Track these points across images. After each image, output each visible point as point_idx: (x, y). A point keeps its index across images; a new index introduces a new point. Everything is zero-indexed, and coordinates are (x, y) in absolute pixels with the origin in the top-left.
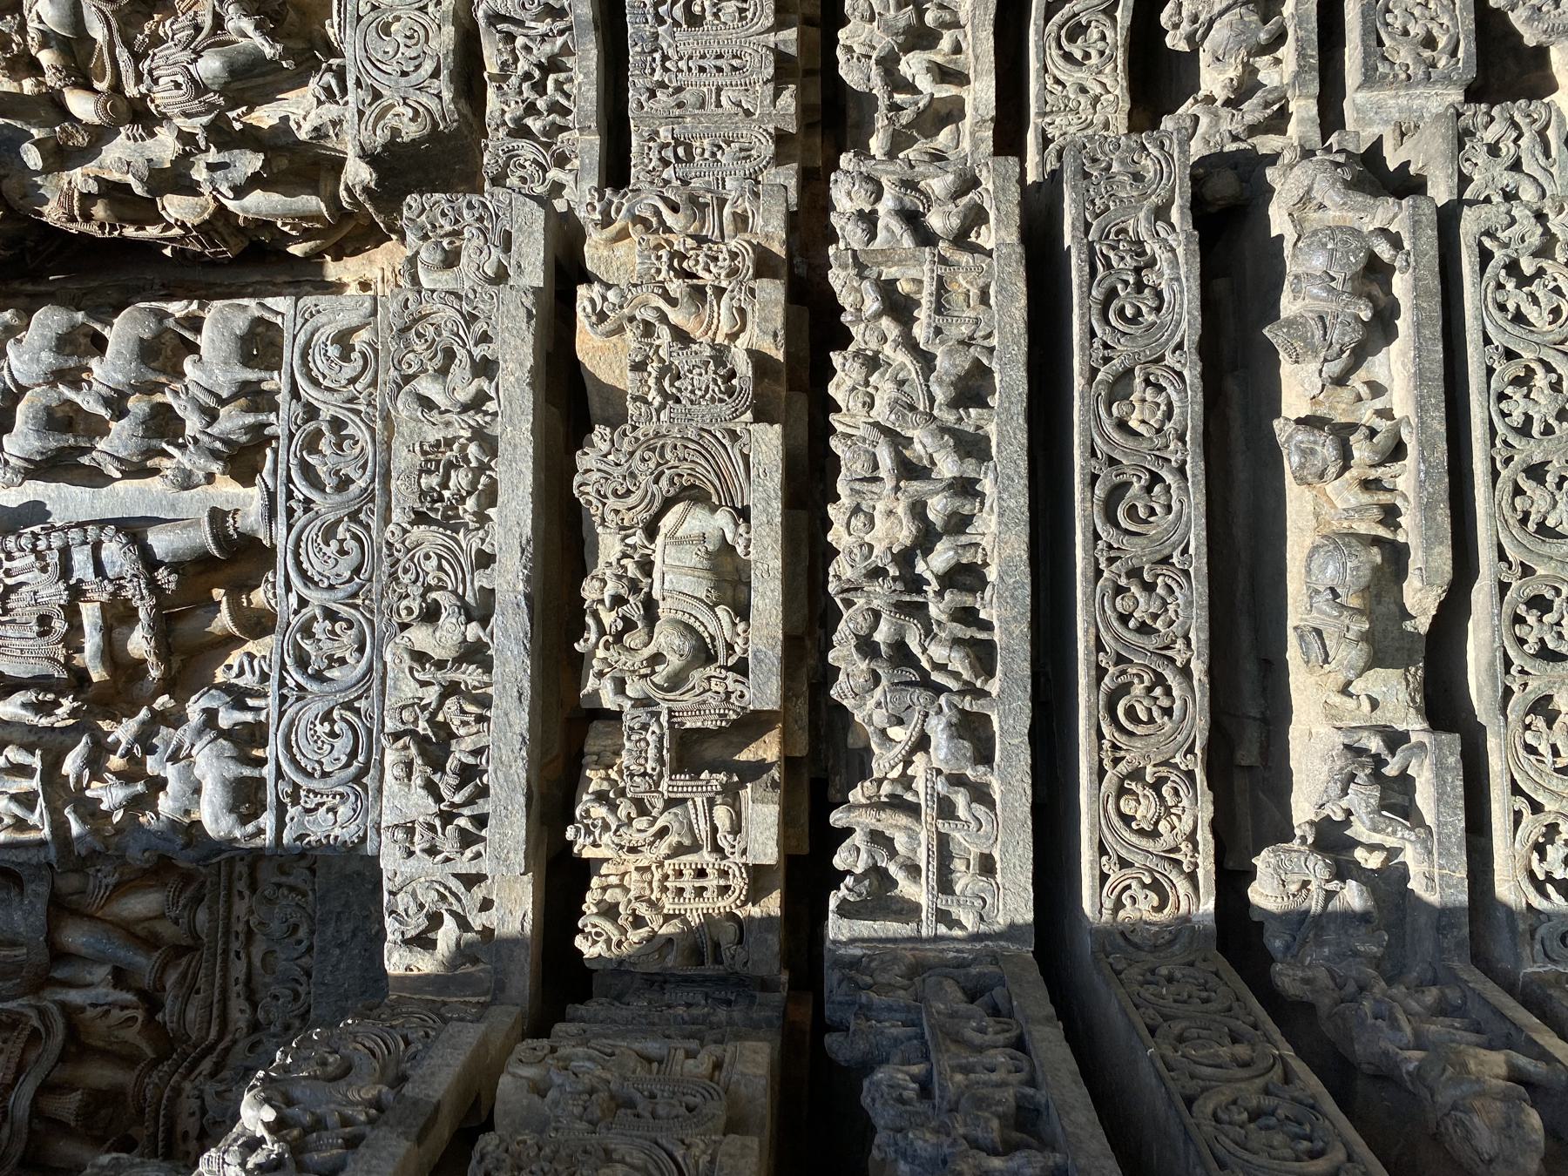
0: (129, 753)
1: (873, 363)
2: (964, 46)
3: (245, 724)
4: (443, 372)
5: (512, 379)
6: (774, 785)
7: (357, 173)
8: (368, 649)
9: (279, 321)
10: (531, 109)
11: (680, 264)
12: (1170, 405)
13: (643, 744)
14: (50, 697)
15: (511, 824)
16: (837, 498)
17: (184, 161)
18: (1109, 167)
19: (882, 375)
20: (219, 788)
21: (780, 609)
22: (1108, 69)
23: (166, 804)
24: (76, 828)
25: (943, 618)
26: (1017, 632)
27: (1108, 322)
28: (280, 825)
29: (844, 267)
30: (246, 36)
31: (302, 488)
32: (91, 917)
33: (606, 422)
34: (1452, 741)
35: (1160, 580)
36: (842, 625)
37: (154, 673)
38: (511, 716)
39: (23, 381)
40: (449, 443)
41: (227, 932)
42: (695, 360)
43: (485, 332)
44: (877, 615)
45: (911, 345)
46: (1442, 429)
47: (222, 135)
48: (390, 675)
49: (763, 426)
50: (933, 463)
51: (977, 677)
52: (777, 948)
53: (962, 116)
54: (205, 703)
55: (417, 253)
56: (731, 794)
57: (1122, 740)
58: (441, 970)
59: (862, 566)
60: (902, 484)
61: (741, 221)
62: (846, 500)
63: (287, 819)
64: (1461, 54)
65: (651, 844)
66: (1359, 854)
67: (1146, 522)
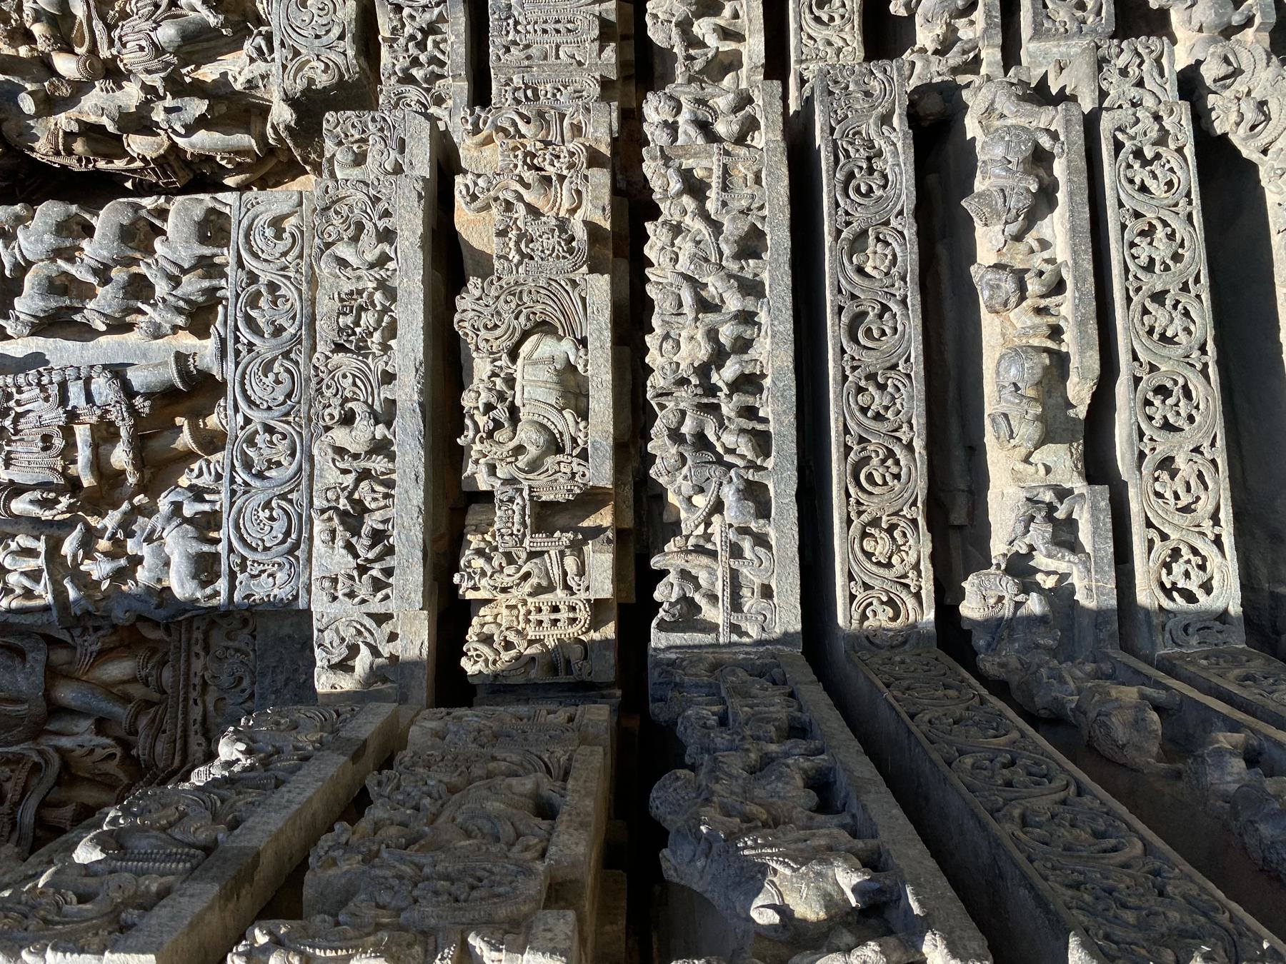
0: (113, 537)
1: (677, 230)
2: (741, 13)
3: (204, 513)
4: (355, 239)
7: (282, 114)
8: (298, 454)
9: (227, 210)
10: (415, 62)
12: (895, 256)
14: (52, 495)
15: (412, 572)
16: (652, 330)
17: (145, 106)
18: (847, 87)
19: (684, 238)
20: (184, 560)
22: (847, 28)
23: (143, 575)
24: (72, 594)
27: (848, 197)
28: (232, 588)
29: (654, 158)
30: (195, 10)
31: (246, 335)
32: (78, 679)
34: (1103, 491)
35: (889, 382)
36: (658, 422)
37: (132, 480)
38: (411, 492)
39: (30, 257)
40: (360, 293)
41: (186, 686)
42: (543, 229)
44: (683, 413)
45: (705, 216)
46: (1090, 267)
47: (177, 86)
48: (317, 466)
49: (596, 276)
50: (723, 301)
52: (613, 662)
53: (740, 65)
54: (172, 498)
55: (334, 155)
56: (577, 548)
57: (863, 498)
58: (358, 688)
59: (671, 379)
61: (577, 130)
62: (659, 331)
63: (237, 583)
64: (1103, 14)
65: (518, 585)
66: (1039, 577)
67: (878, 340)
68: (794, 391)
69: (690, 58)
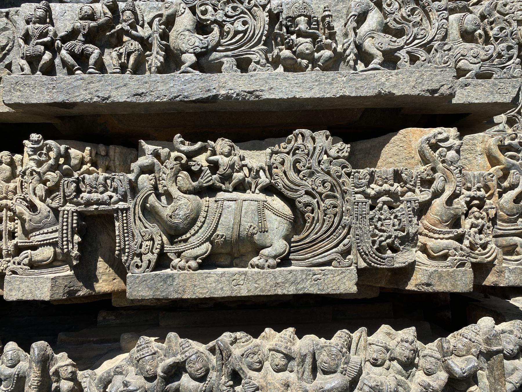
4: (386, 29)
5: (383, 79)
11: (475, 205)
13: (101, 189)
15: (42, 92)
16: (300, 334)
19: (399, 373)
21: (207, 296)
33: (352, 153)
38: (124, 89)
40: (332, 36)
42: (405, 221)
43: (418, 59)
44: (202, 379)
49: (355, 276)
55: (471, 12)
65: (24, 199)
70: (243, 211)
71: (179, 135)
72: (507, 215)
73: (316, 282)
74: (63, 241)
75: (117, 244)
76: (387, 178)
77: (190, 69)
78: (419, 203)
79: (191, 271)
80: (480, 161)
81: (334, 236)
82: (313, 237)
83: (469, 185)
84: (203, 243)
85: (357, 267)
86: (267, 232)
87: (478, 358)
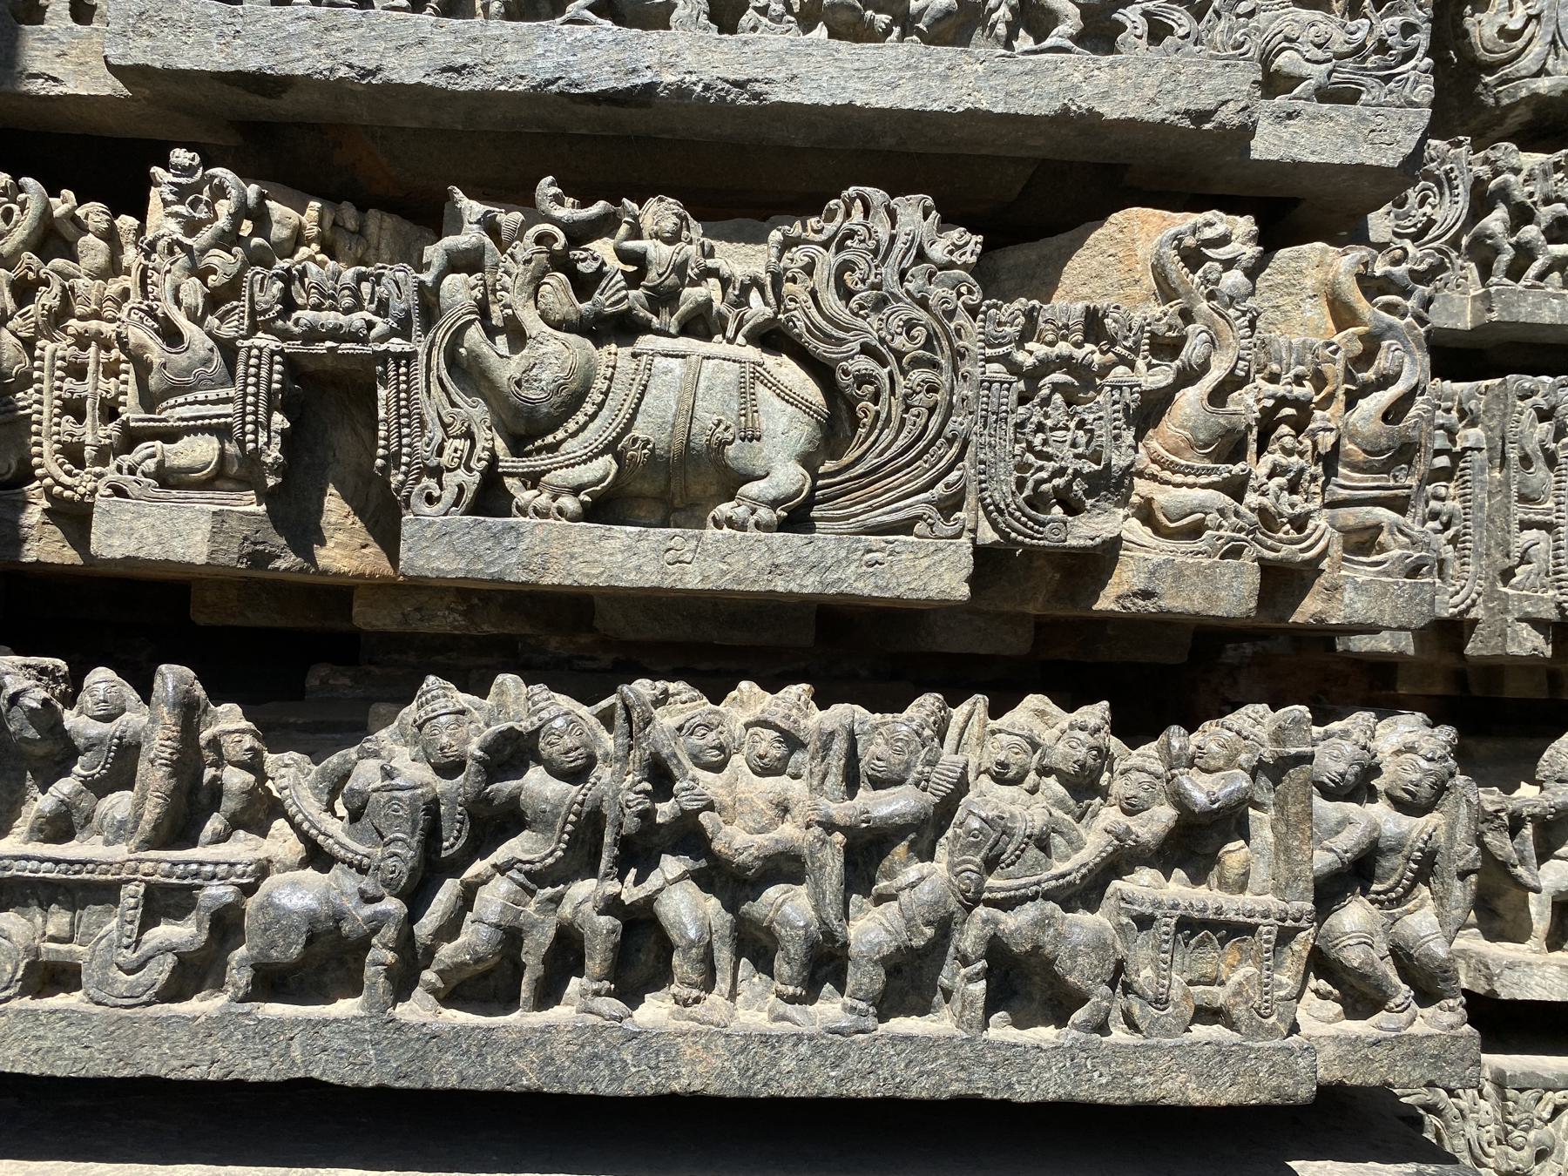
5: (1078, 77)
6: (259, 559)
13: (347, 301)
15: (205, 44)
16: (823, 701)
19: (1060, 804)
25: (566, 910)
26: (521, 1065)
29: (1279, 736)
36: (564, 702)
42: (1103, 433)
43: (1170, 31)
44: (577, 775)
45: (1120, 861)
49: (967, 563)
50: (881, 899)
51: (440, 973)
59: (679, 752)
60: (838, 837)
61: (1363, 542)
62: (817, 720)
65: (151, 313)
68: (605, 1089)
69: (1515, 824)
70: (702, 385)
71: (550, 179)
72: (1365, 451)
73: (871, 569)
74: (244, 424)
75: (382, 443)
76: (1066, 326)
77: (589, 15)
78: (1141, 393)
79: (564, 521)
80: (1309, 314)
81: (926, 462)
82: (871, 461)
83: (1275, 367)
84: (596, 456)
85: (974, 540)
86: (758, 439)
87: (1254, 779)
